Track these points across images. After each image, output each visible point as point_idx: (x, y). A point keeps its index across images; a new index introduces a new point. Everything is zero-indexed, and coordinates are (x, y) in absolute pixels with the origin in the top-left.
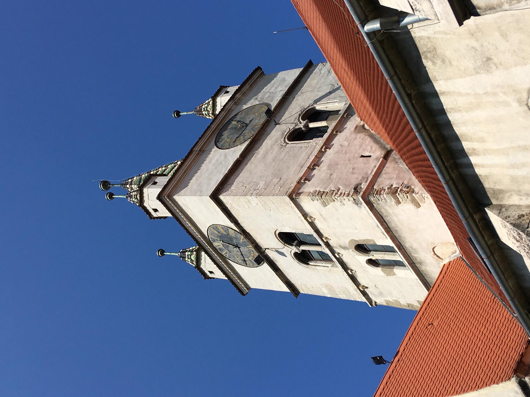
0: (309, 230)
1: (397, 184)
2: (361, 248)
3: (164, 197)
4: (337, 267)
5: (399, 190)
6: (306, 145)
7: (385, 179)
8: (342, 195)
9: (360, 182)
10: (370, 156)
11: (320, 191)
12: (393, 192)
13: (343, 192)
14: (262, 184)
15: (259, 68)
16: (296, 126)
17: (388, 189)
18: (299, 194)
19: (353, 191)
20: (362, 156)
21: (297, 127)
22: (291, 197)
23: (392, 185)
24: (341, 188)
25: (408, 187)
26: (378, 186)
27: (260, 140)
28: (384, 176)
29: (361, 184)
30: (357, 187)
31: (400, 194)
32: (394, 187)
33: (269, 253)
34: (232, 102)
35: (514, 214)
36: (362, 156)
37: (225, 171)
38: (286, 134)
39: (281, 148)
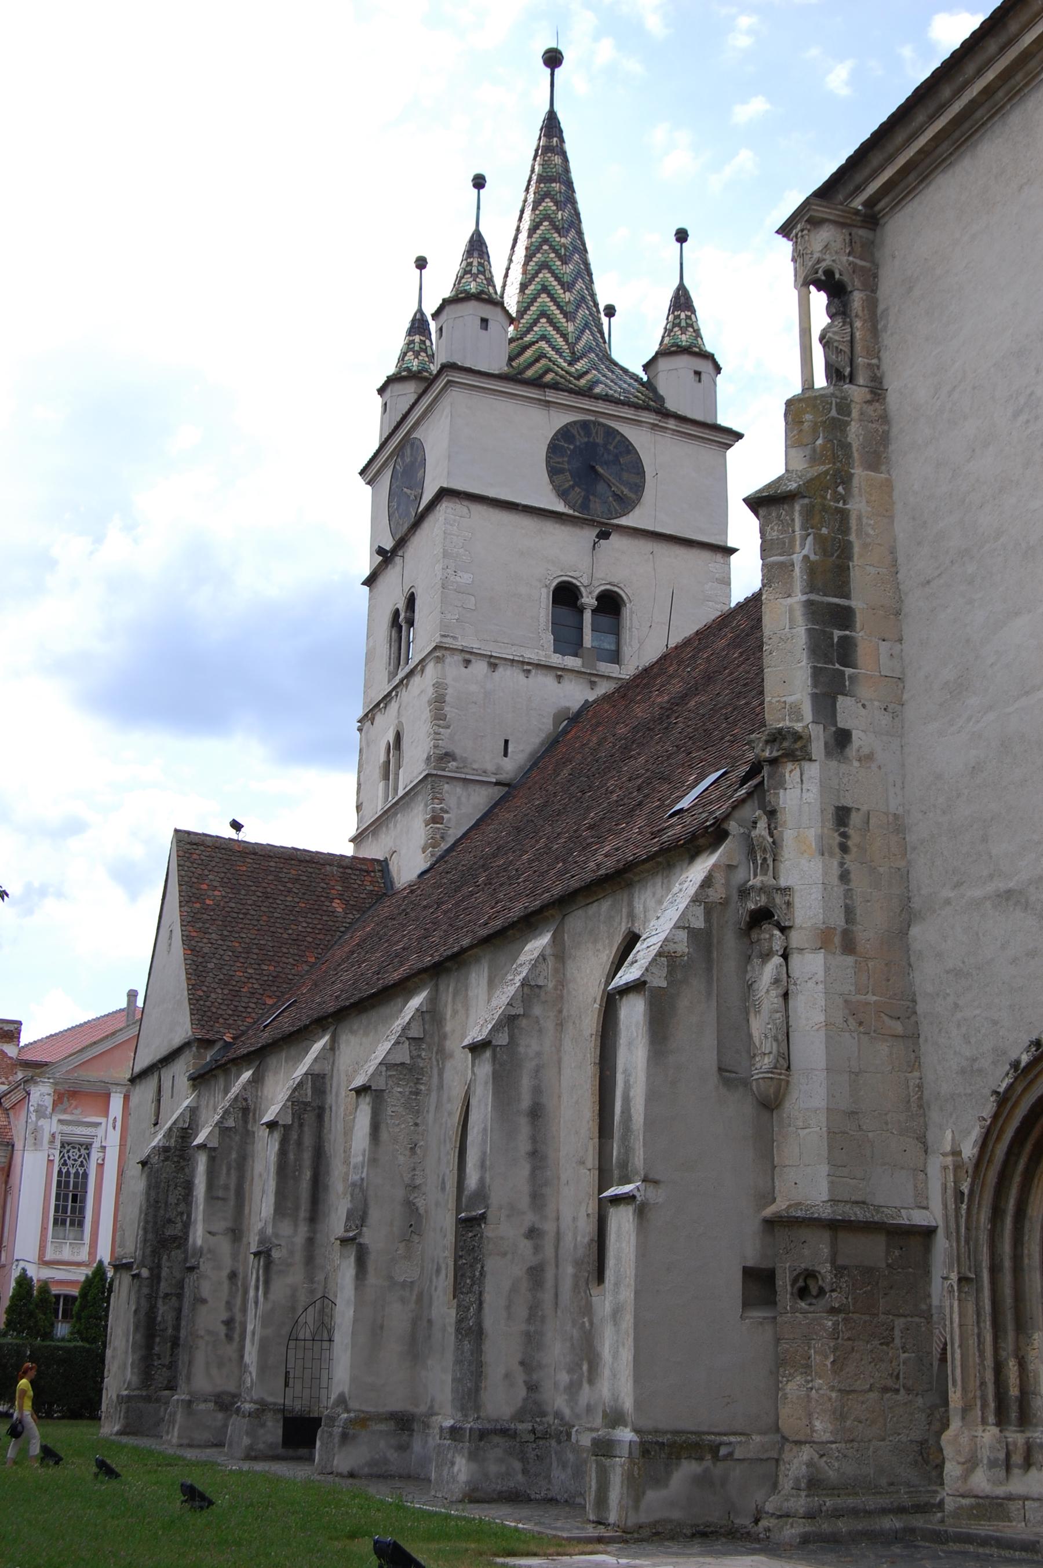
0: (415, 658)
1: (449, 819)
2: (398, 737)
3: (447, 375)
4: (389, 682)
5: (438, 826)
6: (542, 626)
7: (459, 798)
8: (438, 737)
9: (458, 757)
10: (506, 754)
11: (443, 696)
12: (436, 819)
13: (443, 737)
14: (465, 578)
15: (739, 436)
16: (585, 586)
17: (441, 809)
18: (439, 660)
19: (444, 751)
20: (506, 742)
21: (582, 589)
22: (436, 648)
23: (447, 812)
24: (449, 731)
25: (442, 838)
26: (447, 792)
27: (563, 524)
28: (465, 794)
29: (454, 760)
30: (450, 756)
31: (431, 830)
32: (446, 816)
33: (398, 560)
34: (656, 420)
35: (248, 1095)
36: (506, 742)
37: (491, 493)
38: (570, 574)
39: (540, 581)
